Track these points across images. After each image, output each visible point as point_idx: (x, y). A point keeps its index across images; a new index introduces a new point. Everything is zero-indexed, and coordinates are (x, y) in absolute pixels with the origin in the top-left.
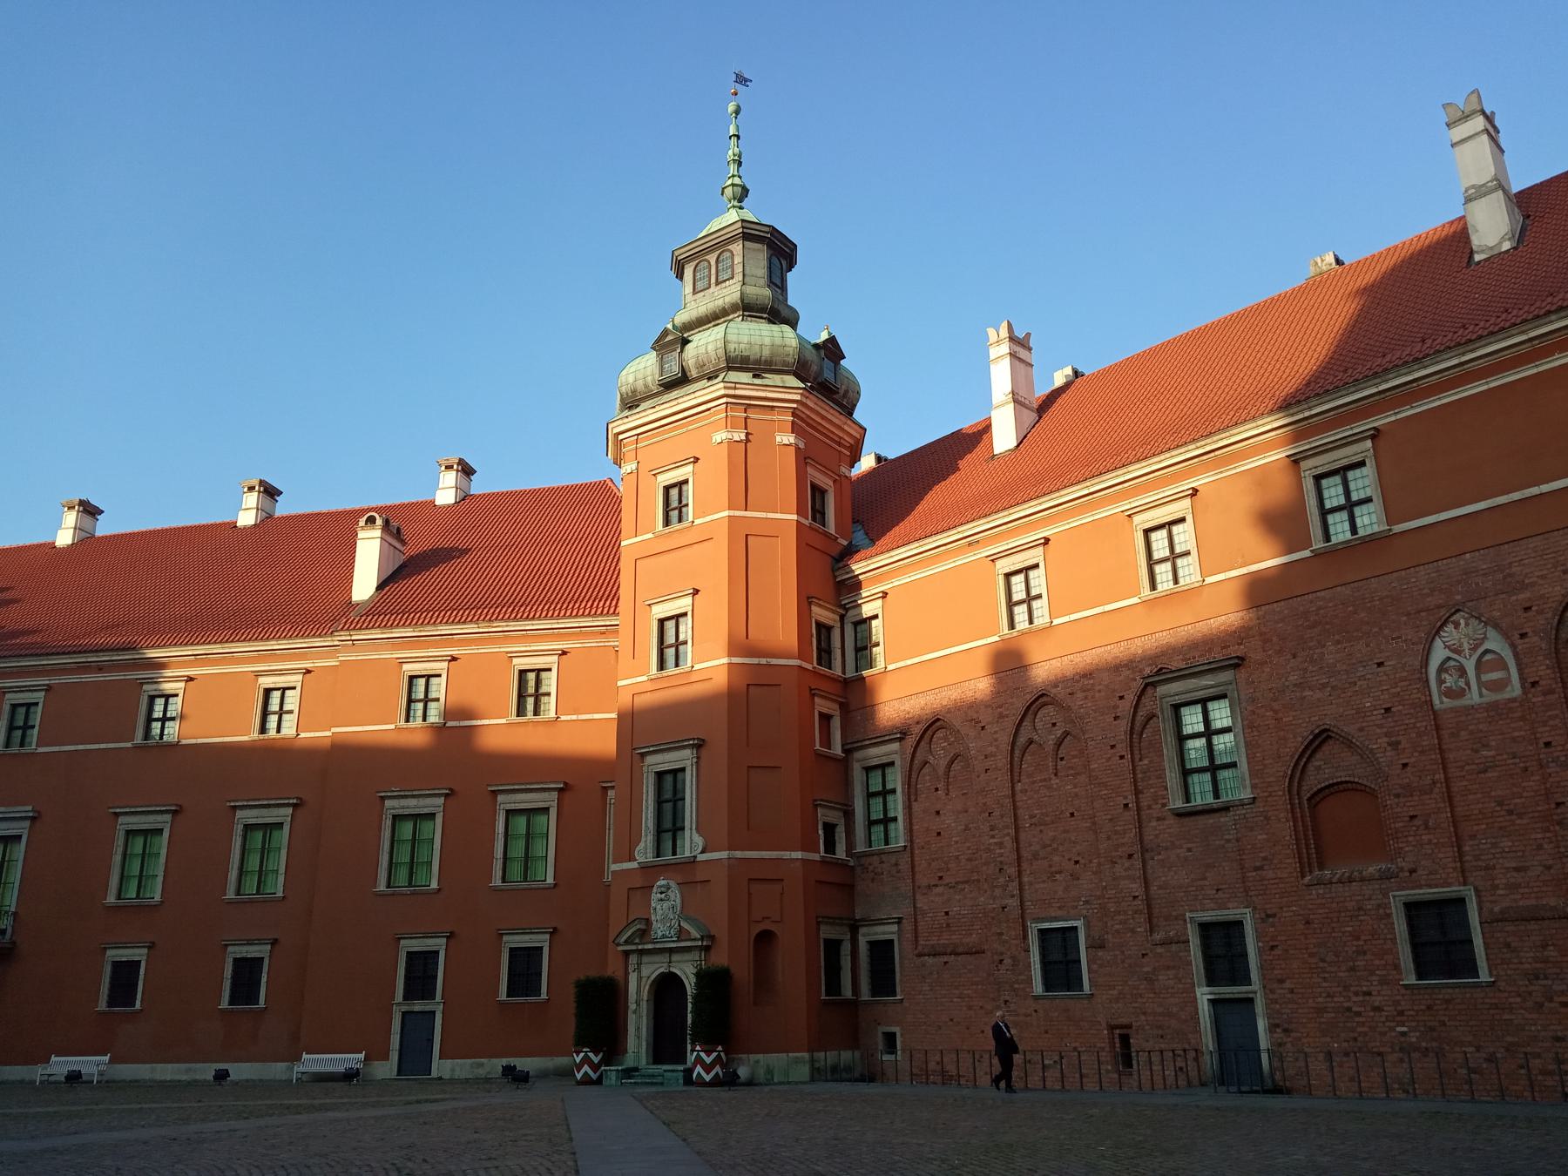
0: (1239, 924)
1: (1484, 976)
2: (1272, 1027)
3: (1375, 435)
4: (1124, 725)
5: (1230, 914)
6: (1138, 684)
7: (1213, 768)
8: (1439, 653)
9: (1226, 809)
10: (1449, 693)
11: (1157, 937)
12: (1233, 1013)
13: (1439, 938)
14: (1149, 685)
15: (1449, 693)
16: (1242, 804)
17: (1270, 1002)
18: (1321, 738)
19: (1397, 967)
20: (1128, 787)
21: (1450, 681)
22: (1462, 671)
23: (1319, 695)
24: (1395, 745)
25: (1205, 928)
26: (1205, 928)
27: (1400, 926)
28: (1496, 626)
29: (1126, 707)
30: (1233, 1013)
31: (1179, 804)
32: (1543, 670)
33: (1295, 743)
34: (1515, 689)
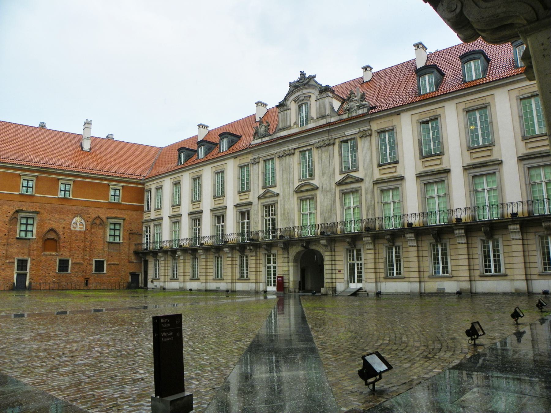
0: (27, 261)
1: (69, 272)
2: (30, 279)
3: (74, 181)
4: (8, 218)
5: (25, 258)
6: (15, 210)
7: (26, 231)
8: (74, 221)
9: (29, 239)
10: (74, 227)
11: (7, 261)
12: (22, 277)
13: (63, 265)
14: (17, 212)
15: (74, 227)
16: (33, 239)
17: (30, 274)
18: (52, 230)
19: (55, 269)
20: (6, 231)
21: (74, 225)
22: (77, 224)
23: (52, 222)
24: (64, 234)
25: (19, 260)
26: (19, 260)
27: (58, 263)
28: (84, 219)
29: (10, 214)
30: (22, 277)
31: (18, 236)
32: (89, 227)
33: (46, 230)
34: (84, 229)
